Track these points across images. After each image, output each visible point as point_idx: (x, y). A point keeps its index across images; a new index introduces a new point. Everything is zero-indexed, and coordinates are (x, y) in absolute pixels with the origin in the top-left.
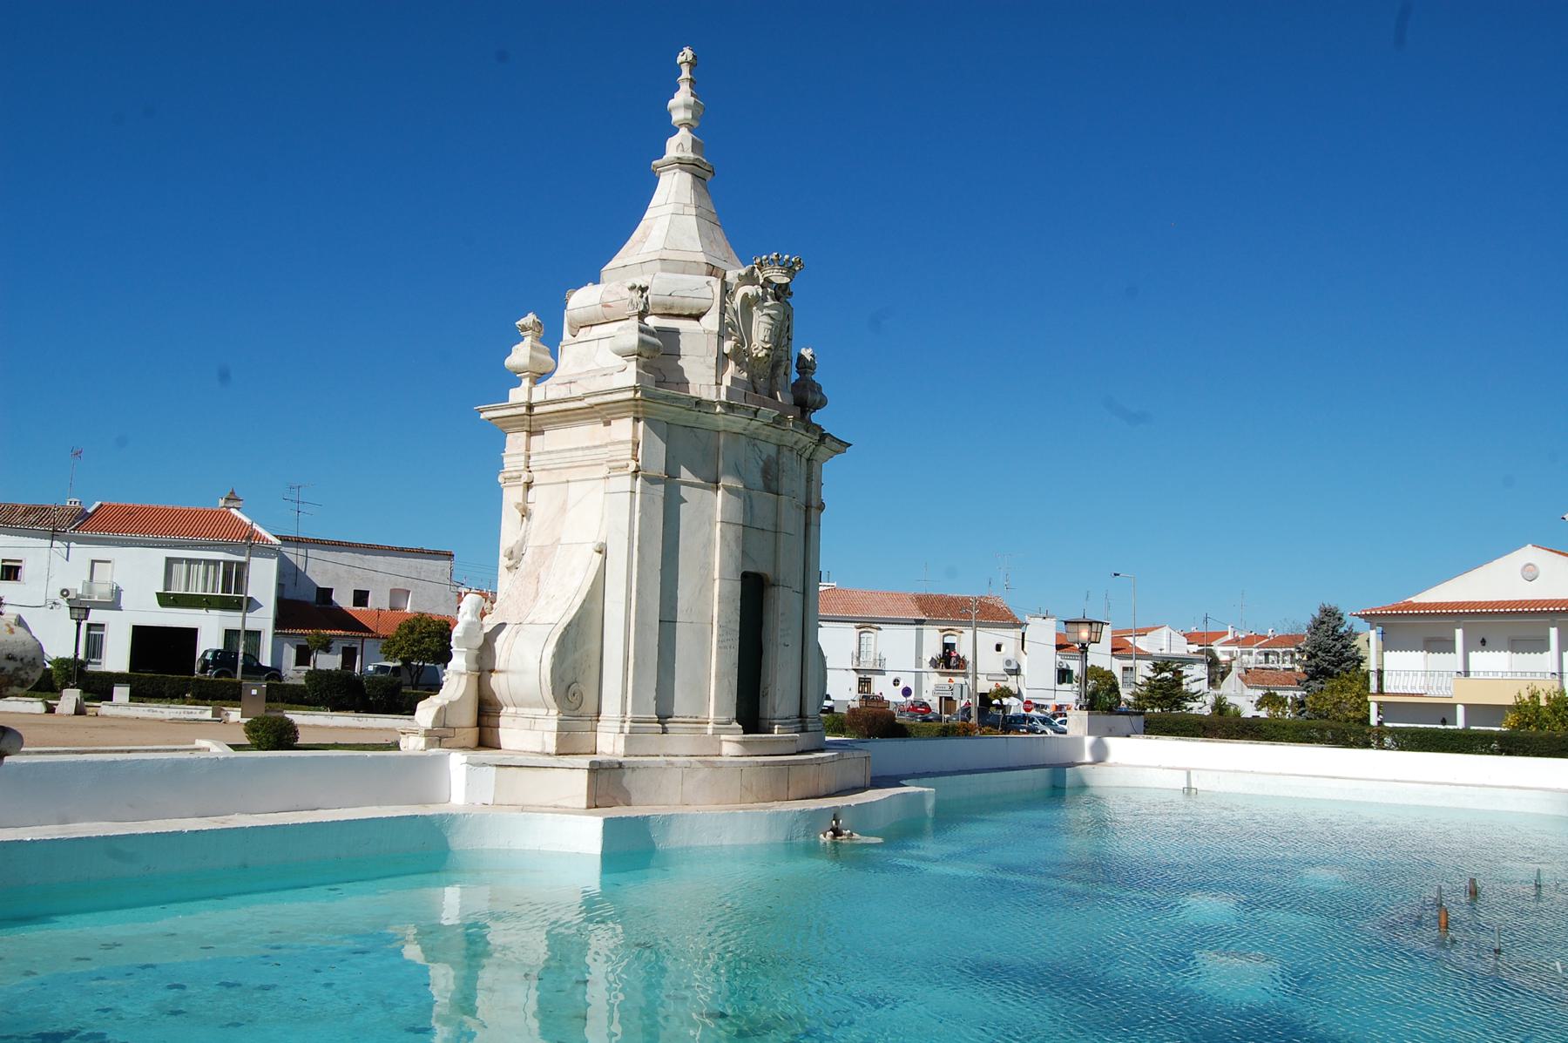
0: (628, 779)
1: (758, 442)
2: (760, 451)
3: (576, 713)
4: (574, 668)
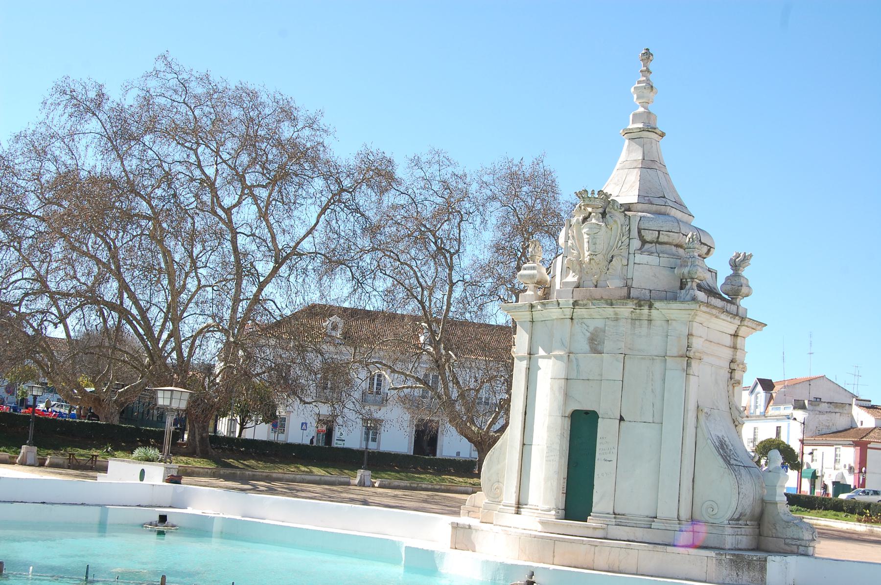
0: (474, 535)
1: (585, 320)
2: (588, 326)
3: (497, 500)
4: (498, 474)
